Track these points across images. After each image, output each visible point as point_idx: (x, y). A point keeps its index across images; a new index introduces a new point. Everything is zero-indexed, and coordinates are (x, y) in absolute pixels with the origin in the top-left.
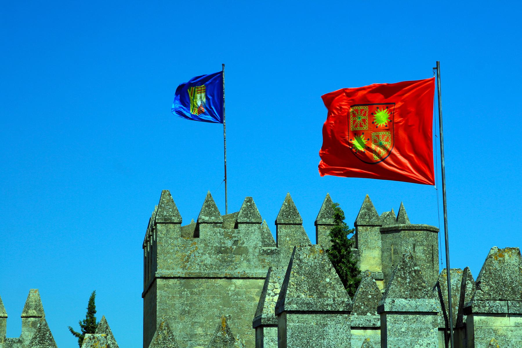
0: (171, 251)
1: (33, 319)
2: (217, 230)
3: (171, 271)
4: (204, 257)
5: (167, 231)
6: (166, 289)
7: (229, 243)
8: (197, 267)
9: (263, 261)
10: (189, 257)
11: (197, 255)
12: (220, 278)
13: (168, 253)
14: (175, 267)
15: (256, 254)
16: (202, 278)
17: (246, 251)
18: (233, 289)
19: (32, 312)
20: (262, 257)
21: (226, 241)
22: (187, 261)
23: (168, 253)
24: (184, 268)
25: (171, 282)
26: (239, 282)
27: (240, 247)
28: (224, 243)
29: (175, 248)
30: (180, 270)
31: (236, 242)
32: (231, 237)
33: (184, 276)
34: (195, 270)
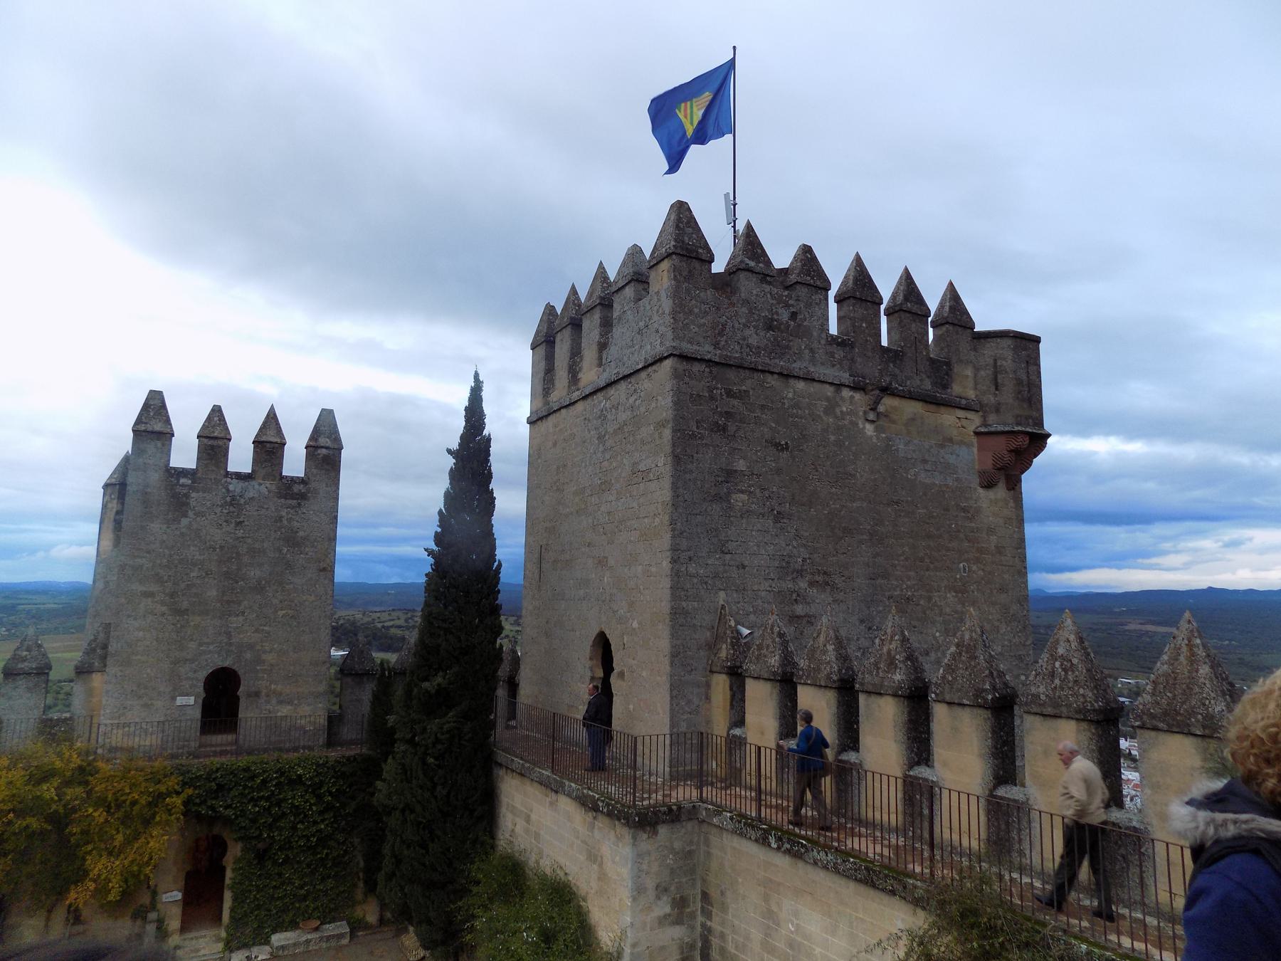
0: (696, 310)
1: (324, 451)
2: (767, 288)
3: (695, 347)
4: (747, 332)
5: (690, 272)
6: (687, 379)
8: (737, 348)
10: (724, 326)
11: (737, 325)
12: (772, 373)
13: (691, 312)
14: (702, 340)
15: (823, 342)
16: (745, 368)
18: (790, 395)
19: (323, 441)
21: (780, 311)
22: (721, 334)
24: (716, 345)
25: (697, 367)
26: (801, 385)
27: (799, 325)
28: (777, 313)
29: (703, 307)
30: (708, 347)
31: (794, 316)
32: (787, 306)
33: (717, 360)
34: (735, 352)
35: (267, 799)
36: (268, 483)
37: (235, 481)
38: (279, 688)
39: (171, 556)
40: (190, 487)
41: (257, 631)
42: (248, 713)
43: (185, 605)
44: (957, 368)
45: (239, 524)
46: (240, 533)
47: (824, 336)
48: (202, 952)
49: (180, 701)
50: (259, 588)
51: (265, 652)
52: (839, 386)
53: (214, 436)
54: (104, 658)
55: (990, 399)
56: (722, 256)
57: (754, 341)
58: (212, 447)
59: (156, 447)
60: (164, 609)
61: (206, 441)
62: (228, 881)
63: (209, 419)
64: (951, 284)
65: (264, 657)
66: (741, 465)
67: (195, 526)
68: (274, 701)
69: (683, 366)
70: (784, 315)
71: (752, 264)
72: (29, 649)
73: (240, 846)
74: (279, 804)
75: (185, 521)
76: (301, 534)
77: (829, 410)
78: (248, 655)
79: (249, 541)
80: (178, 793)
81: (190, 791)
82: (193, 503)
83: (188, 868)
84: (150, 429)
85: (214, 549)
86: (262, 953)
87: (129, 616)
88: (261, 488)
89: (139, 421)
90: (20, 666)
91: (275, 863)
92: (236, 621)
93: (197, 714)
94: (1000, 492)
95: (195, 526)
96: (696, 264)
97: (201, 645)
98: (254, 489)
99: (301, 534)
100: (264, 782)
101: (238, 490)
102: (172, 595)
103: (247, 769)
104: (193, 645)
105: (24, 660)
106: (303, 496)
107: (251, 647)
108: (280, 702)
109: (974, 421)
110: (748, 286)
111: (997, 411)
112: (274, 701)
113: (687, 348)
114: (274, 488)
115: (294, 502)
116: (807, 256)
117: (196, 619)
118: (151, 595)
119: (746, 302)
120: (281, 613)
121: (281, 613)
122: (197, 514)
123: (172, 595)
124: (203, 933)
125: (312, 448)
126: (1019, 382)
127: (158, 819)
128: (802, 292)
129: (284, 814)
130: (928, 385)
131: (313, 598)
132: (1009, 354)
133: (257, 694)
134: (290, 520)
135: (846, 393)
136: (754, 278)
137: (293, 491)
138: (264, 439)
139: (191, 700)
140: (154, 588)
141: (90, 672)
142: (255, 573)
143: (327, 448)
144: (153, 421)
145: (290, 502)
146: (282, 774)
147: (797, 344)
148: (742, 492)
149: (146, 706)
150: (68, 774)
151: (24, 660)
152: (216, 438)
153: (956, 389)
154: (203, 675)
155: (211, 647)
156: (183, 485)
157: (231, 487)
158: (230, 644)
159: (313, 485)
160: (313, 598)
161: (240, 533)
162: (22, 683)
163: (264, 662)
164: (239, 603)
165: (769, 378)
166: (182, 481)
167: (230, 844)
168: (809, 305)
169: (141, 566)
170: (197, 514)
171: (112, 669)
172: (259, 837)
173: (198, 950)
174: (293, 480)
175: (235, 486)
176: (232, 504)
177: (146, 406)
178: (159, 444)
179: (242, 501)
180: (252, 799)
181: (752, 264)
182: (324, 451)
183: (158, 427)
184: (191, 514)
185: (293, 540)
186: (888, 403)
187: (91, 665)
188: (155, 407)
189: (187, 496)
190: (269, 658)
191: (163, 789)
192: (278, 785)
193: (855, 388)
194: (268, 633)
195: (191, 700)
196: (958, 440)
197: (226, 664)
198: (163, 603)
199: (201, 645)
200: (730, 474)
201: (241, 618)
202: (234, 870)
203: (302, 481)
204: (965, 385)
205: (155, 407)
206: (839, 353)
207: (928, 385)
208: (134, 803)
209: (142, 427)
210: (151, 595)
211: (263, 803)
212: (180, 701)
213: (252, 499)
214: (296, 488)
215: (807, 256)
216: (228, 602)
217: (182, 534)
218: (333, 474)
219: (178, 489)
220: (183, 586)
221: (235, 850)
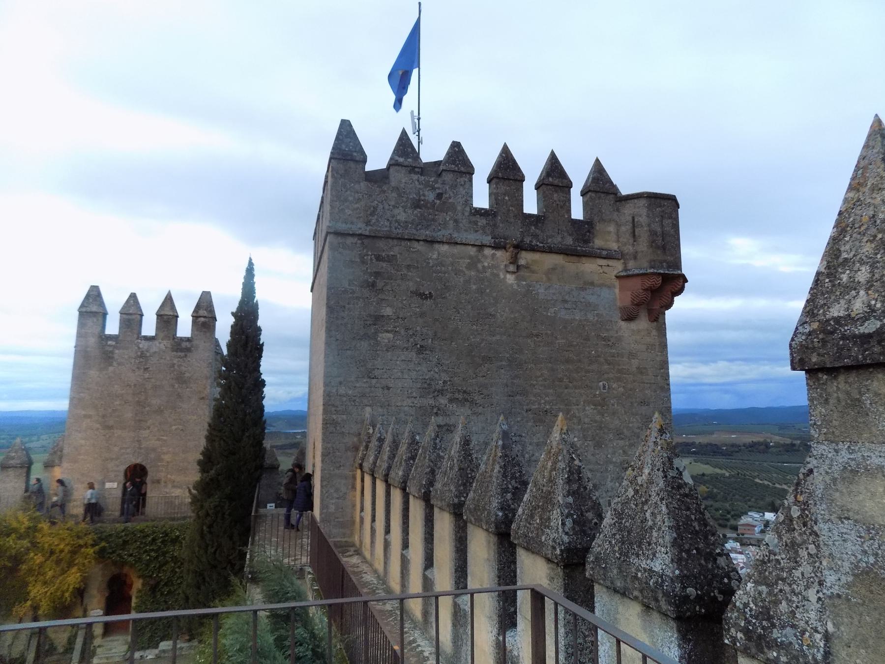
0: (351, 198)
1: (202, 319)
2: (415, 177)
3: (349, 226)
4: (396, 211)
5: (346, 170)
6: (341, 250)
7: (431, 196)
8: (387, 223)
9: (476, 223)
10: (375, 208)
11: (387, 207)
12: (418, 241)
13: (346, 200)
14: (355, 220)
15: (467, 214)
16: (393, 239)
17: (453, 208)
18: (435, 256)
19: (202, 312)
20: (473, 219)
21: (426, 193)
22: (373, 214)
23: (346, 200)
24: (368, 223)
26: (445, 248)
27: (444, 203)
28: (424, 195)
29: (356, 196)
30: (361, 225)
31: (439, 196)
32: (433, 188)
33: (367, 233)
34: (384, 226)
35: (156, 551)
36: (165, 342)
37: (143, 342)
38: (173, 477)
40: (115, 347)
41: (158, 440)
42: (153, 494)
43: (111, 423)
44: (599, 227)
45: (146, 369)
46: (147, 375)
47: (468, 209)
48: (113, 651)
49: (108, 485)
50: (159, 411)
51: (164, 453)
52: (481, 247)
53: (132, 312)
54: (61, 458)
55: (629, 249)
56: (378, 158)
57: (402, 217)
58: (129, 320)
60: (98, 426)
62: (133, 605)
63: (128, 301)
64: (597, 160)
65: (162, 456)
66: (388, 311)
68: (170, 486)
69: (340, 239)
70: (431, 196)
71: (401, 160)
72: (16, 452)
73: (141, 581)
74: (164, 554)
75: (111, 369)
76: (187, 375)
77: (470, 267)
78: (152, 456)
79: (153, 380)
80: (93, 546)
81: (103, 544)
82: (116, 356)
83: (107, 595)
84: (89, 309)
85: (130, 386)
86: (150, 654)
88: (162, 345)
89: (82, 306)
91: (162, 594)
92: (145, 433)
93: (119, 493)
94: (643, 323)
96: (352, 164)
97: (121, 449)
98: (156, 346)
99: (187, 375)
100: (154, 540)
101: (146, 348)
102: (104, 416)
103: (142, 531)
104: (116, 449)
106: (188, 350)
107: (154, 450)
108: (174, 487)
109: (617, 266)
110: (399, 177)
111: (635, 258)
112: (170, 486)
113: (342, 227)
114: (169, 346)
115: (183, 354)
116: (456, 151)
117: (117, 432)
118: (90, 417)
119: (396, 189)
120: (174, 427)
121: (174, 427)
122: (119, 364)
124: (115, 638)
125: (195, 317)
126: (653, 233)
127: (77, 561)
128: (448, 177)
129: (166, 563)
130: (569, 241)
131: (195, 417)
132: (644, 212)
133: (158, 481)
134: (179, 366)
135: (488, 252)
136: (403, 170)
137: (182, 347)
138: (162, 313)
139: (115, 485)
140: (92, 412)
141: (53, 466)
142: (155, 402)
143: (205, 317)
144: (92, 306)
145: (179, 354)
146: (167, 535)
147: (440, 217)
148: (388, 332)
150: (22, 531)
151: (13, 458)
153: (598, 242)
154: (123, 468)
155: (128, 451)
156: (110, 346)
157: (141, 346)
158: (140, 448)
159: (195, 342)
160: (195, 417)
161: (147, 375)
162: (11, 472)
163: (161, 460)
164: (146, 421)
165: (415, 244)
166: (109, 343)
167: (135, 579)
168: (454, 187)
170: (119, 364)
172: (151, 576)
173: (111, 649)
174: (181, 339)
175: (144, 345)
176: (141, 357)
177: (88, 296)
179: (148, 354)
180: (146, 551)
181: (401, 160)
182: (202, 319)
183: (94, 308)
184: (115, 364)
185: (181, 379)
186: (526, 257)
187: (53, 461)
188: (94, 296)
189: (112, 352)
190: (167, 458)
191: (81, 542)
192: (162, 542)
193: (496, 247)
194: (165, 441)
195: (115, 485)
196: (604, 284)
197: (138, 461)
199: (121, 449)
200: (378, 319)
201: (148, 431)
202: (137, 597)
203: (188, 340)
204: (607, 238)
205: (94, 296)
206: (482, 222)
207: (569, 241)
208: (62, 551)
209: (84, 310)
210: (90, 417)
211: (153, 554)
212: (108, 485)
213: (155, 352)
214: (184, 345)
215: (456, 151)
216: (140, 421)
218: (208, 334)
219: (107, 348)
220: (110, 410)
221: (138, 584)
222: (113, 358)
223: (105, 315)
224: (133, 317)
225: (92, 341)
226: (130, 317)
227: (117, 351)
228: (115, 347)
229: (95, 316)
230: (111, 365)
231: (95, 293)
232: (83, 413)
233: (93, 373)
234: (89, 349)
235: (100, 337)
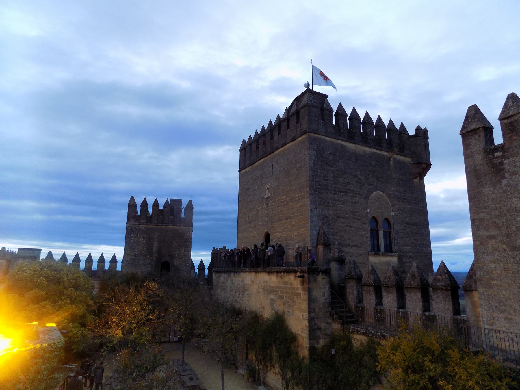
39: (500, 208)
58: (511, 124)
59: (476, 139)
60: (504, 246)
61: (505, 121)
67: (512, 183)
72: (441, 275)
75: (504, 182)
82: (506, 167)
84: (469, 129)
87: (483, 253)
89: (463, 128)
90: (438, 284)
95: (512, 183)
102: (508, 236)
105: (439, 281)
118: (493, 237)
123: (508, 236)
149: (507, 319)
151: (439, 281)
152: (512, 116)
156: (498, 157)
166: (496, 154)
169: (483, 219)
171: (481, 290)
178: (477, 137)
184: (507, 175)
187: (471, 286)
189: (502, 164)
198: (502, 242)
210: (493, 237)
217: (505, 191)
219: (495, 161)
220: (514, 228)
222: (504, 169)
223: (492, 128)
224: (516, 118)
225: (479, 158)
226: (512, 120)
227: (506, 161)
228: (503, 157)
229: (476, 134)
230: (504, 177)
231: (473, 112)
232: (487, 234)
233: (487, 190)
234: (478, 168)
235: (486, 151)
